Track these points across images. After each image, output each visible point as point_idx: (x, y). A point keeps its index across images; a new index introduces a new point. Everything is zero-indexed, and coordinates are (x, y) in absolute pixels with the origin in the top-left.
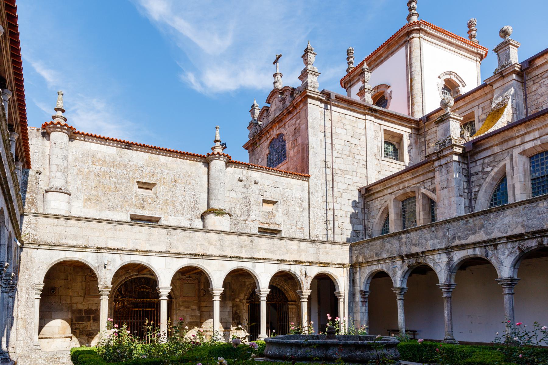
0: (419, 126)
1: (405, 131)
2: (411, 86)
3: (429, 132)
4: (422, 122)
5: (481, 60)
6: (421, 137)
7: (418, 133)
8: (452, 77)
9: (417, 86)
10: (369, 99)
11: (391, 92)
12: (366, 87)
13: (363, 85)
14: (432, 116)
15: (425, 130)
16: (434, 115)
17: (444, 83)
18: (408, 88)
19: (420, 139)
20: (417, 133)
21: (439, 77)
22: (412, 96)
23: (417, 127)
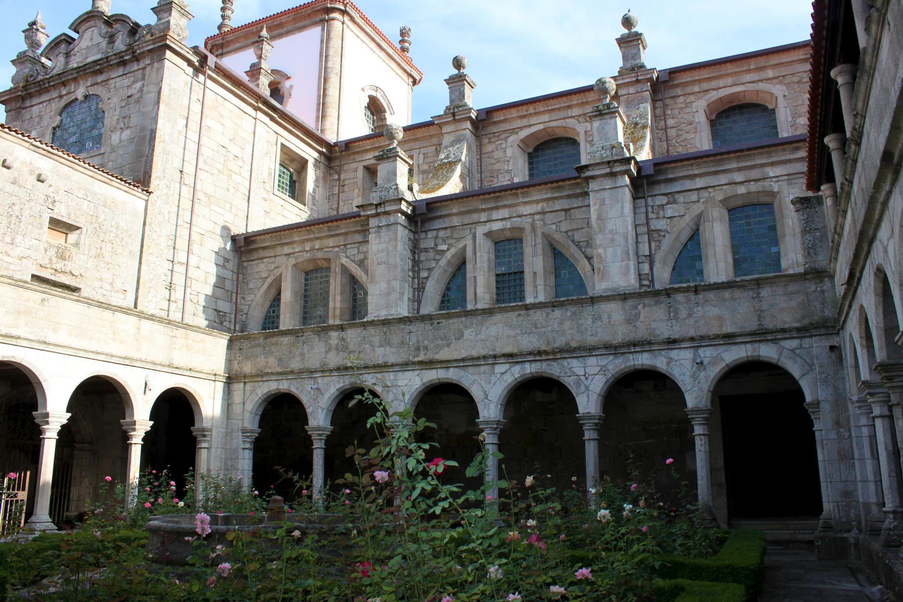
0: (331, 154)
1: (310, 154)
2: (325, 89)
3: (346, 167)
4: (337, 148)
5: (413, 85)
6: (332, 172)
7: (329, 164)
8: (379, 96)
9: (333, 91)
10: (263, 87)
11: (291, 86)
12: (262, 66)
13: (257, 61)
14: (354, 144)
15: (341, 162)
16: (357, 144)
17: (368, 100)
18: (319, 89)
19: (330, 175)
20: (327, 164)
21: (363, 90)
22: (324, 104)
23: (329, 155)
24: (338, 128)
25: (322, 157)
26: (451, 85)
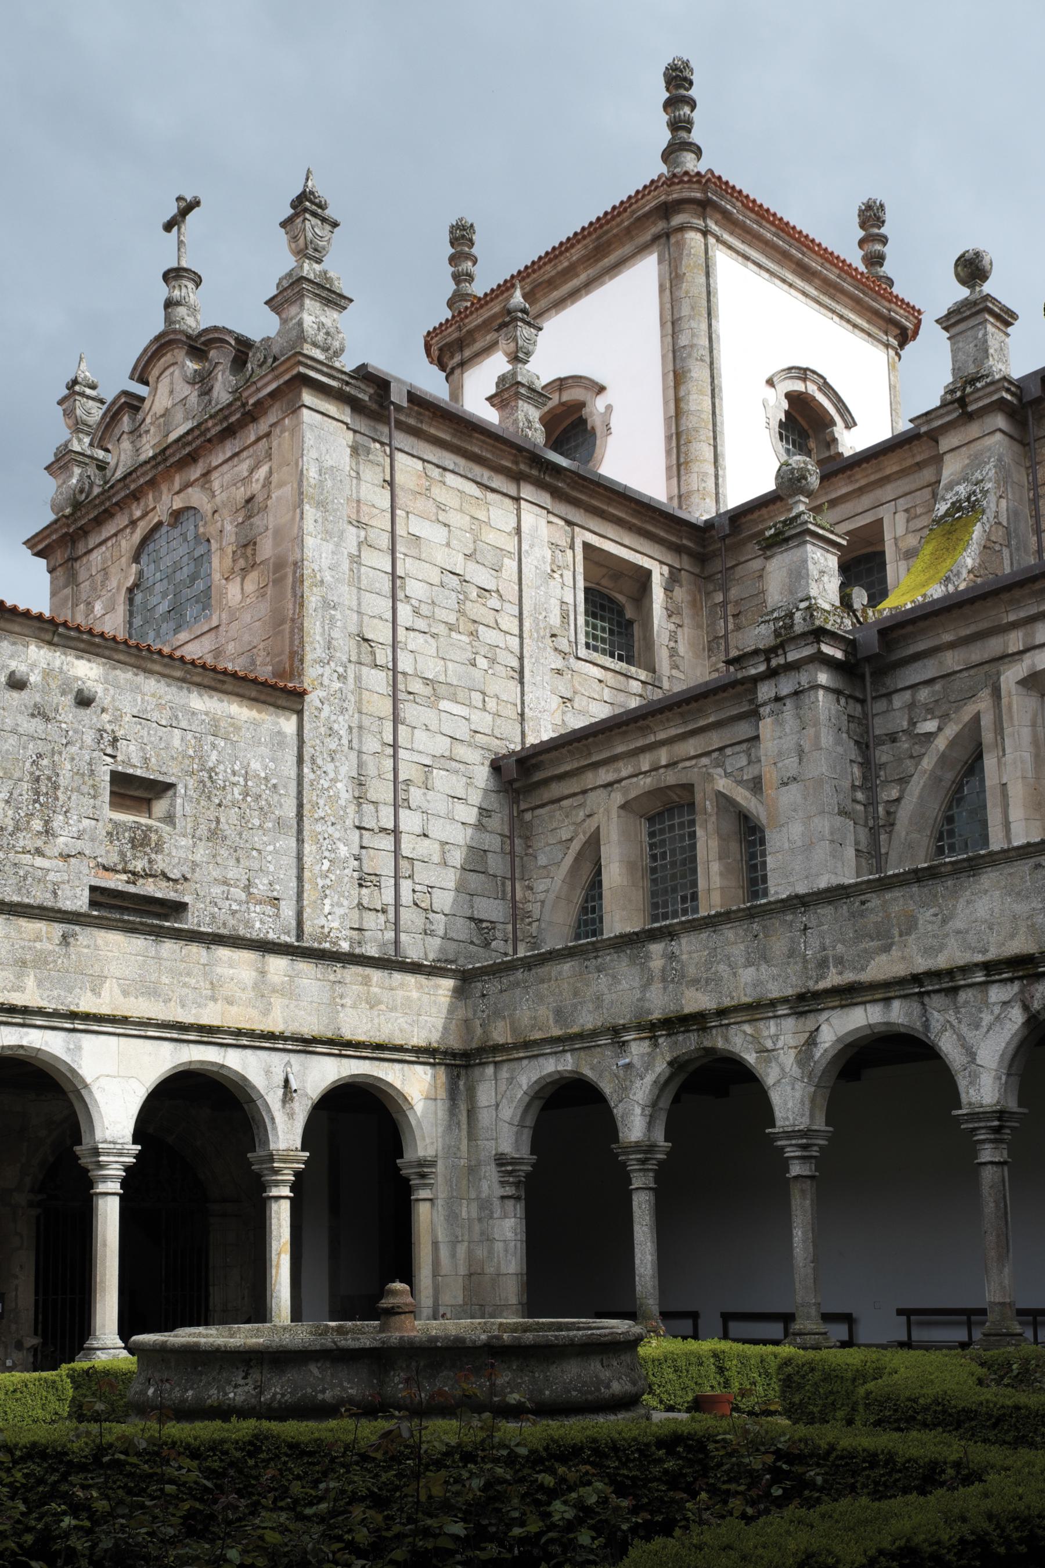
3: (740, 571)
6: (711, 587)
7: (703, 569)
8: (812, 389)
14: (749, 517)
17: (785, 405)
19: (708, 594)
20: (697, 571)
21: (770, 382)
23: (700, 550)
24: (717, 485)
25: (685, 557)
26: (955, 330)
